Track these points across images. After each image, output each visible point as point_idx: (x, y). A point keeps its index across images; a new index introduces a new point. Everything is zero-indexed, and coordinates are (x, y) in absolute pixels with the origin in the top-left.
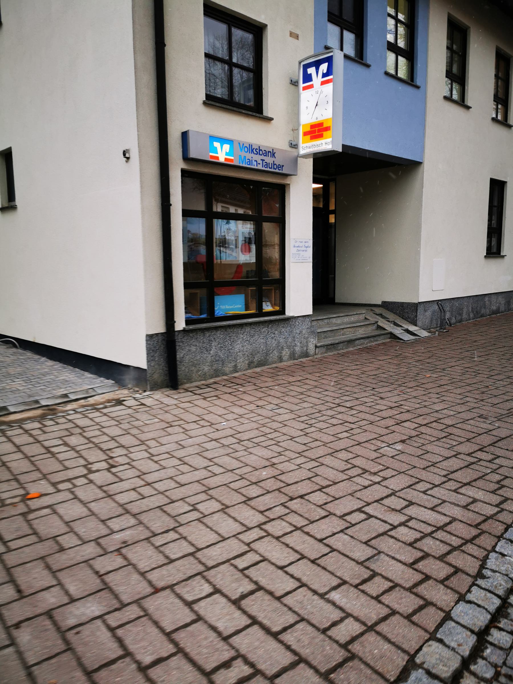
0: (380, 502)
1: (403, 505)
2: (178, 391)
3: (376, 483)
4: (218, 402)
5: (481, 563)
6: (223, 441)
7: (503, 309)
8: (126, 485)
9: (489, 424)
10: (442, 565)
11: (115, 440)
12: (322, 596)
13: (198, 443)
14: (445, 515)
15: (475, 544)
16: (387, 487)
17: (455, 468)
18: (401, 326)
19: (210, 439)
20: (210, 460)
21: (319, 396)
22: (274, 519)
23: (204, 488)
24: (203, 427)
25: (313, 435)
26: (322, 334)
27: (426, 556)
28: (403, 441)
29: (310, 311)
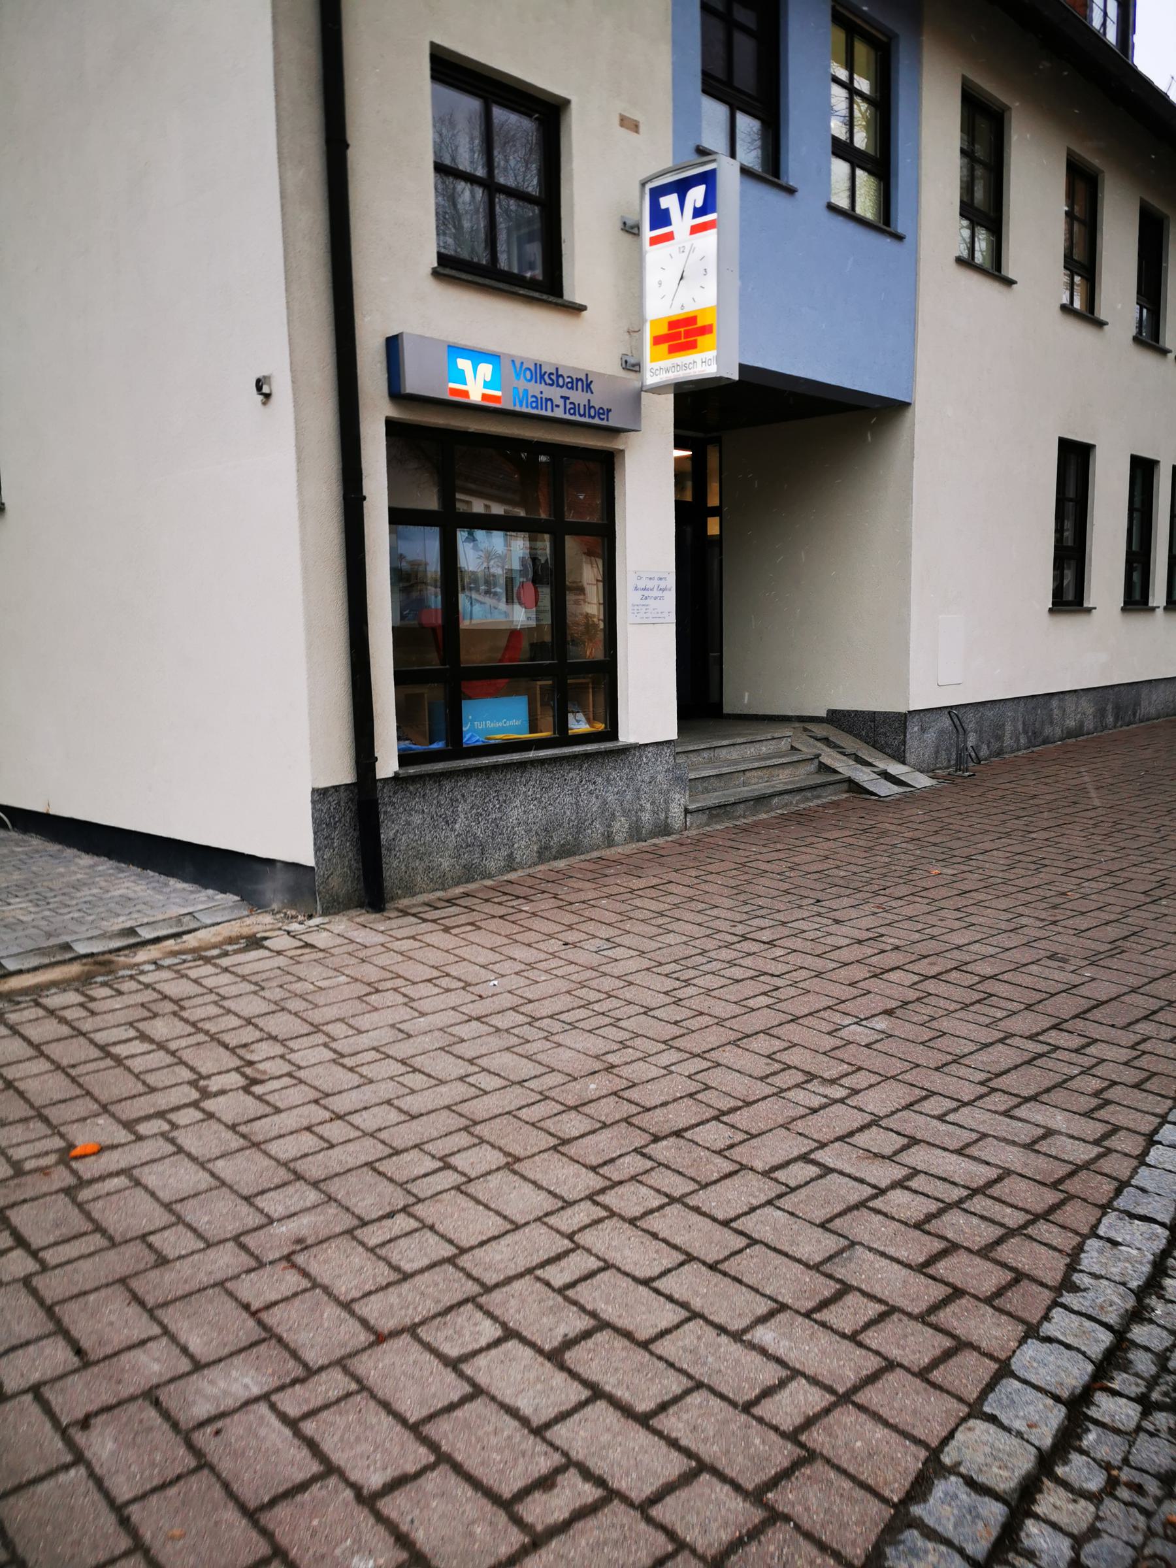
0: (847, 1140)
1: (898, 1146)
2: (385, 914)
3: (835, 1101)
4: (475, 937)
5: (1068, 1260)
6: (496, 1021)
7: (1091, 727)
8: (288, 1121)
9: (1072, 972)
10: (988, 1265)
11: (256, 1026)
12: (737, 1336)
13: (440, 1025)
14: (988, 1163)
15: (1053, 1223)
16: (861, 1110)
17: (1004, 1066)
18: (870, 765)
19: (466, 1018)
20: (471, 1061)
21: (699, 918)
22: (621, 1183)
23: (464, 1122)
24: (448, 990)
25: (695, 1004)
26: (698, 783)
27: (952, 1248)
28: (889, 1012)
29: (671, 733)
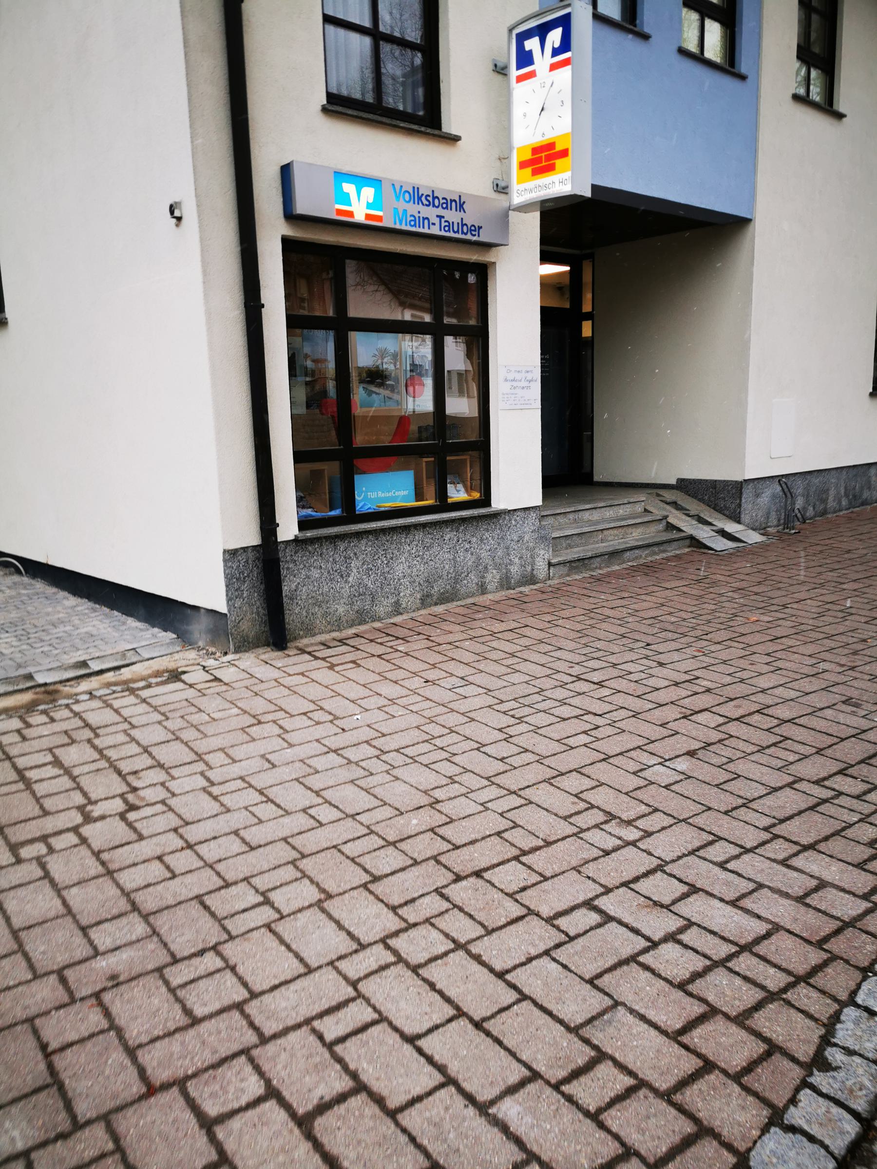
0: (632, 886)
1: (677, 894)
2: (286, 652)
3: (628, 843)
4: (354, 674)
8: (146, 849)
9: (863, 717)
10: (743, 1034)
11: (150, 754)
12: (483, 1108)
14: (759, 917)
15: (813, 987)
16: (650, 854)
17: (789, 812)
18: (710, 524)
20: (317, 793)
21: (543, 659)
22: (415, 925)
24: (318, 723)
25: (522, 741)
26: (562, 540)
27: (712, 1012)
28: (691, 753)
